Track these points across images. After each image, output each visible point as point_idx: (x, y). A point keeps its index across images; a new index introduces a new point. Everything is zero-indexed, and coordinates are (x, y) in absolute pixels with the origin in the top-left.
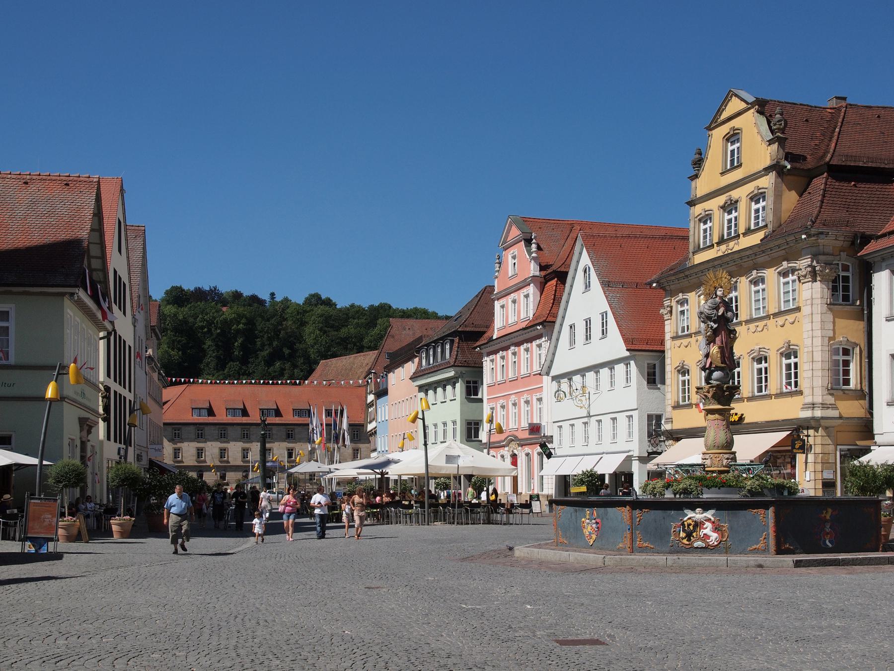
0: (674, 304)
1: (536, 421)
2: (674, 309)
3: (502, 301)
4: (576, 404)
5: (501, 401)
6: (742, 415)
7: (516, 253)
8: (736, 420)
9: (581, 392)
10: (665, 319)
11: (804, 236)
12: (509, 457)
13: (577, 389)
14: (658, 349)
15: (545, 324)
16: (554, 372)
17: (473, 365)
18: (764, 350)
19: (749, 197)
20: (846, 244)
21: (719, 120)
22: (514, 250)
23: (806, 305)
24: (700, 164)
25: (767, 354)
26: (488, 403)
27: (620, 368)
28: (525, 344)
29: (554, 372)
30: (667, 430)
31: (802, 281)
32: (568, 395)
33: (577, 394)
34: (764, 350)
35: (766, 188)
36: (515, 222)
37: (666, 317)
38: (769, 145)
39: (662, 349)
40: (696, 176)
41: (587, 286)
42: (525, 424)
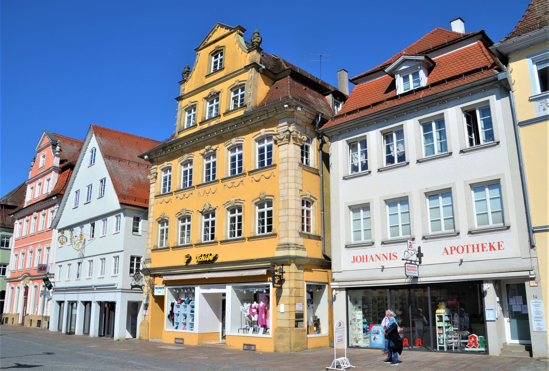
0: (159, 171)
1: (44, 263)
2: (158, 176)
3: (32, 185)
4: (74, 247)
5: (23, 250)
6: (217, 255)
7: (46, 154)
8: (211, 260)
9: (79, 239)
10: (151, 183)
11: (286, 106)
12: (23, 288)
13: (76, 236)
14: (143, 206)
15: (59, 196)
16: (60, 226)
17: (8, 227)
18: (240, 201)
19: (230, 89)
20: (311, 121)
21: (206, 43)
22: (45, 152)
23: (283, 163)
24: (188, 74)
25: (241, 205)
26: (14, 251)
27: (112, 220)
28: (43, 211)
29: (60, 226)
30: (147, 269)
31: (279, 144)
32: (69, 240)
33: (76, 239)
34: (240, 201)
35: (246, 81)
36: (48, 134)
37: (151, 181)
38: (249, 52)
39: (145, 206)
40: (184, 81)
41: (93, 161)
42: (36, 265)
